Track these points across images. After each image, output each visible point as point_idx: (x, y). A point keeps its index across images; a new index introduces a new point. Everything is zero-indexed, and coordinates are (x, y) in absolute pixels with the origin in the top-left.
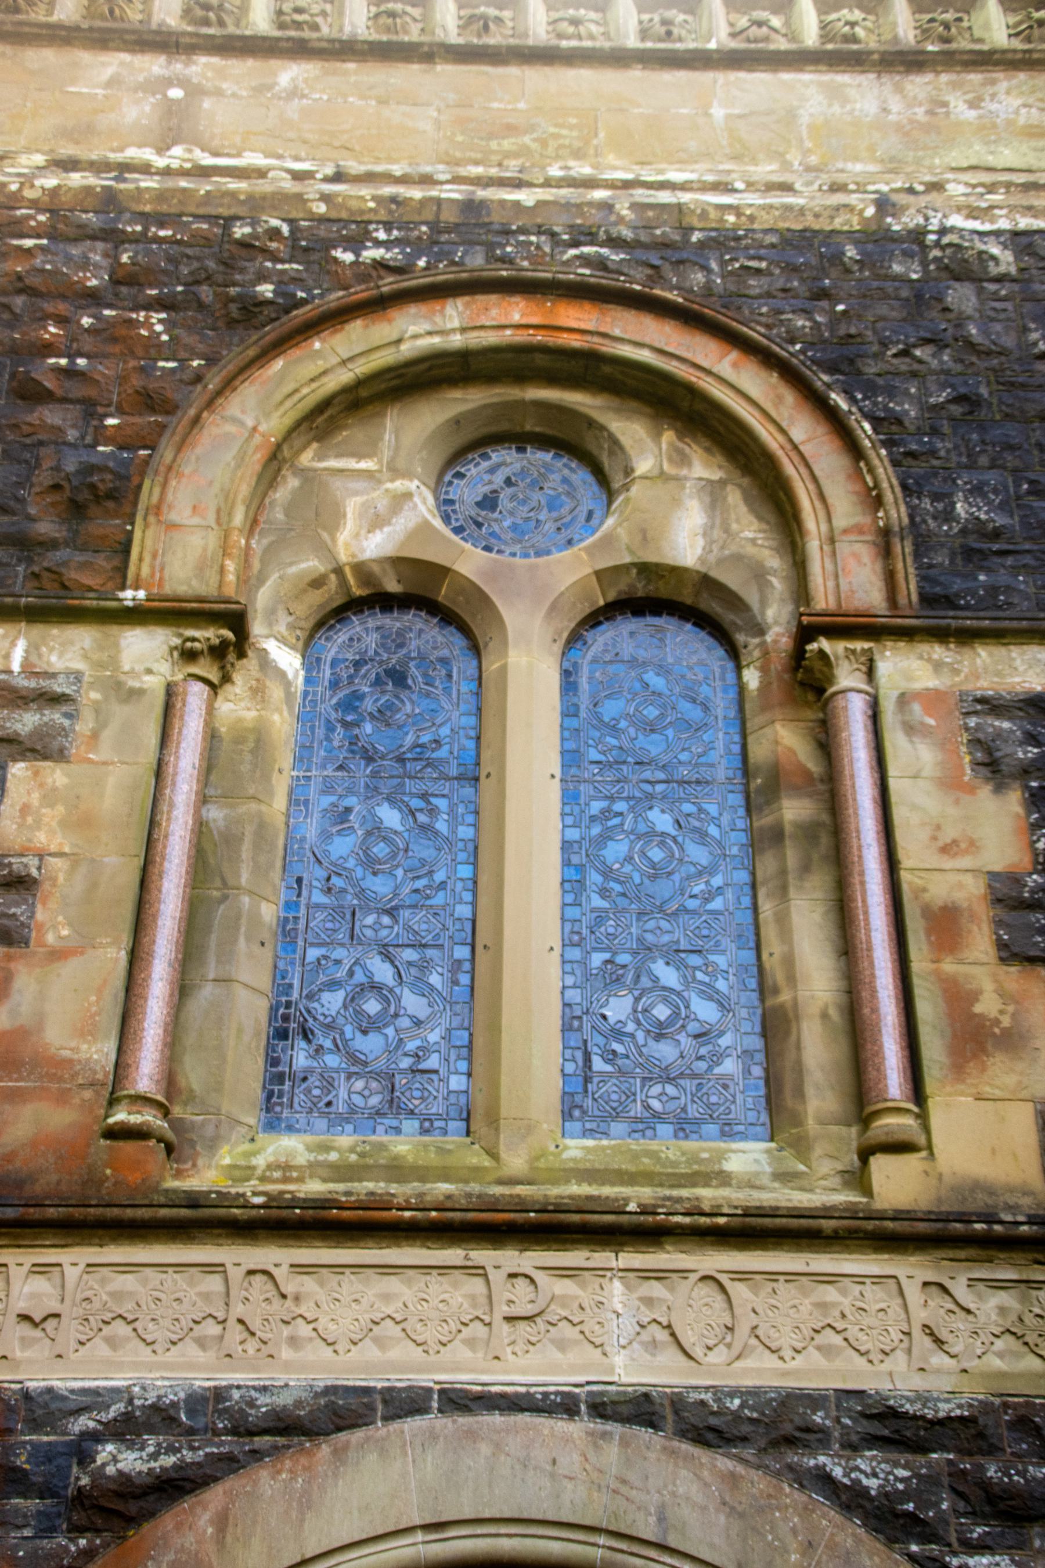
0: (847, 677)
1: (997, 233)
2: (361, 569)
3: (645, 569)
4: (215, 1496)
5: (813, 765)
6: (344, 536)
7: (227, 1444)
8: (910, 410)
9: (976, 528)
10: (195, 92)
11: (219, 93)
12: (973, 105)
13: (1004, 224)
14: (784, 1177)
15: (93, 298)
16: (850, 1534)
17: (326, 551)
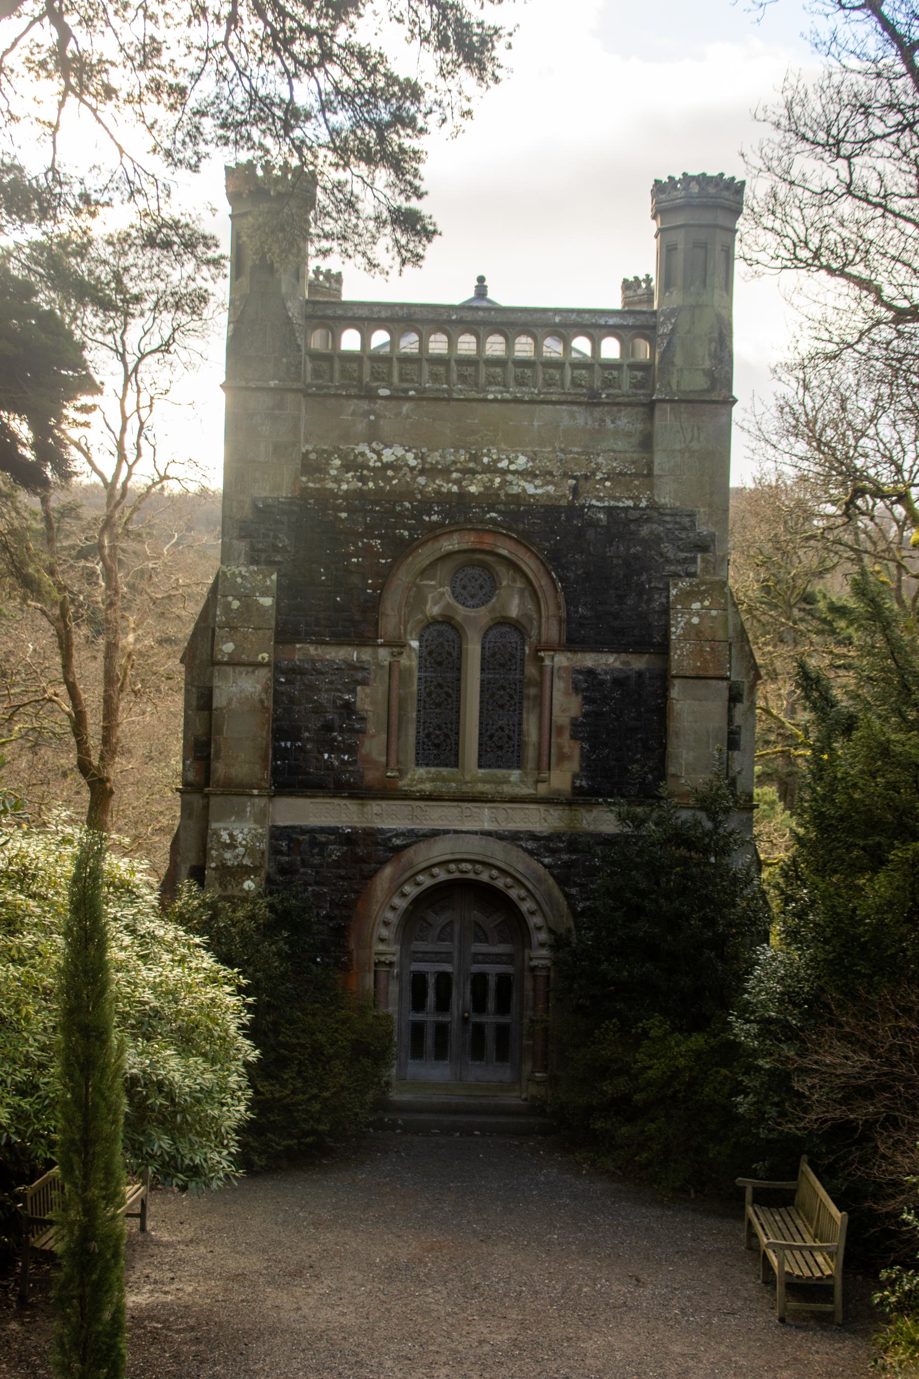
0: (547, 662)
1: (604, 507)
2: (433, 617)
3: (503, 617)
4: (413, 848)
5: (538, 679)
6: (428, 607)
7: (415, 839)
8: (571, 575)
9: (583, 617)
10: (378, 416)
11: (385, 417)
12: (613, 422)
13: (606, 504)
14: (522, 782)
15: (361, 536)
16: (525, 856)
17: (423, 612)
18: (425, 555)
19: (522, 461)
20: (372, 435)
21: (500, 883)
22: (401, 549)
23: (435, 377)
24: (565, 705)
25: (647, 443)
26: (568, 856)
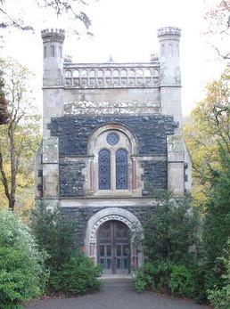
18: (101, 130)
19: (124, 105)
20: (83, 99)
21: (123, 221)
22: (94, 129)
23: (100, 83)
24: (140, 171)
25: (159, 98)
26: (142, 213)
